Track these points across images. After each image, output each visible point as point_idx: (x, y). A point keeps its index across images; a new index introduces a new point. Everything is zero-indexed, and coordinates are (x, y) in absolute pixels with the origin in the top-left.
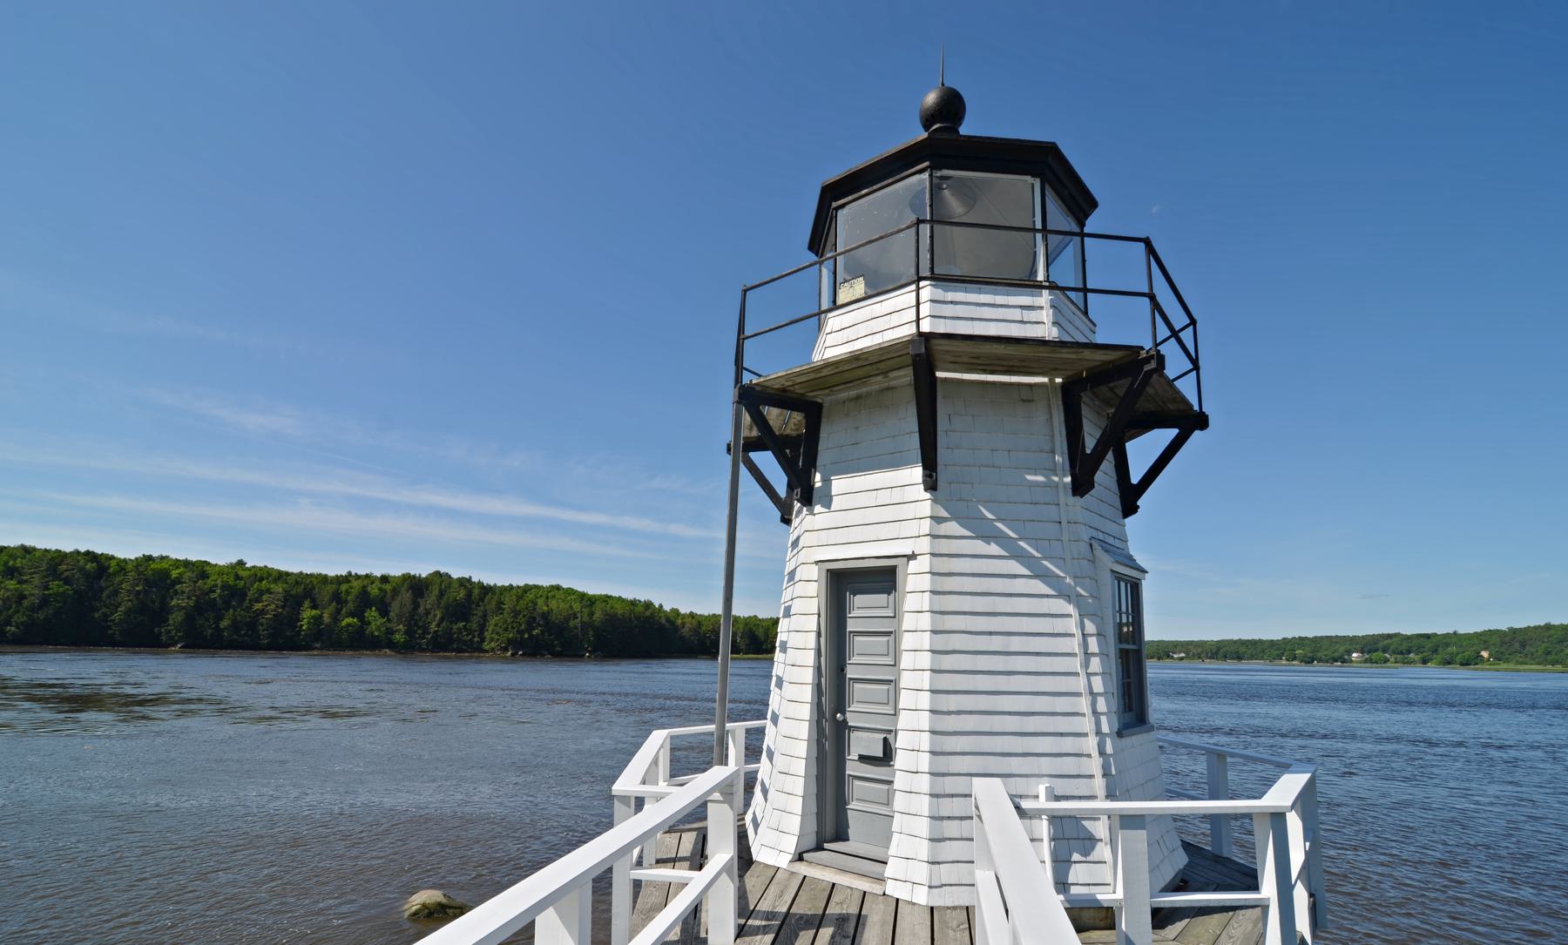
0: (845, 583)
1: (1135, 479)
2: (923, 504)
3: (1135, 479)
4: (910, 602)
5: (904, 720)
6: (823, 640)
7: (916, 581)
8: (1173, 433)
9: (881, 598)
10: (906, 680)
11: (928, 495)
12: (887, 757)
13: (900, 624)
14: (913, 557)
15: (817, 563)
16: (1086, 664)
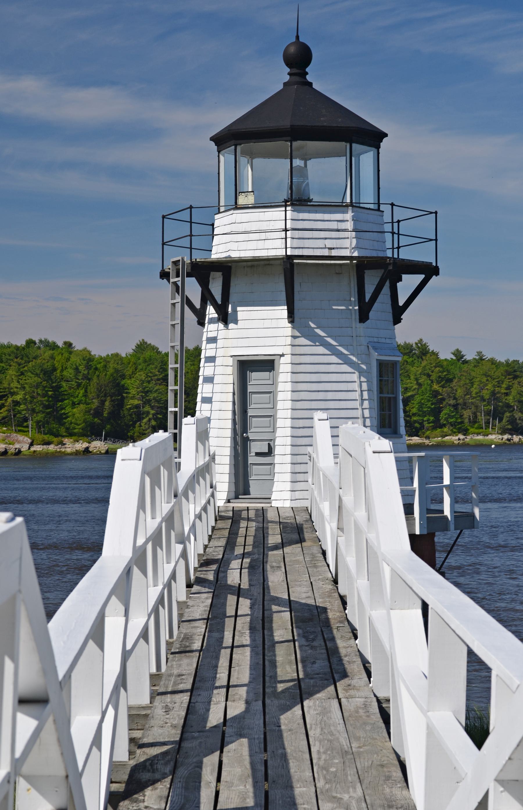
0: (246, 367)
1: (401, 303)
2: (287, 328)
3: (401, 303)
4: (282, 378)
5: (279, 432)
6: (236, 397)
7: (284, 367)
8: (422, 276)
9: (266, 374)
10: (280, 414)
11: (290, 325)
12: (270, 452)
13: (276, 388)
14: (283, 355)
15: (232, 356)
16: (362, 404)
